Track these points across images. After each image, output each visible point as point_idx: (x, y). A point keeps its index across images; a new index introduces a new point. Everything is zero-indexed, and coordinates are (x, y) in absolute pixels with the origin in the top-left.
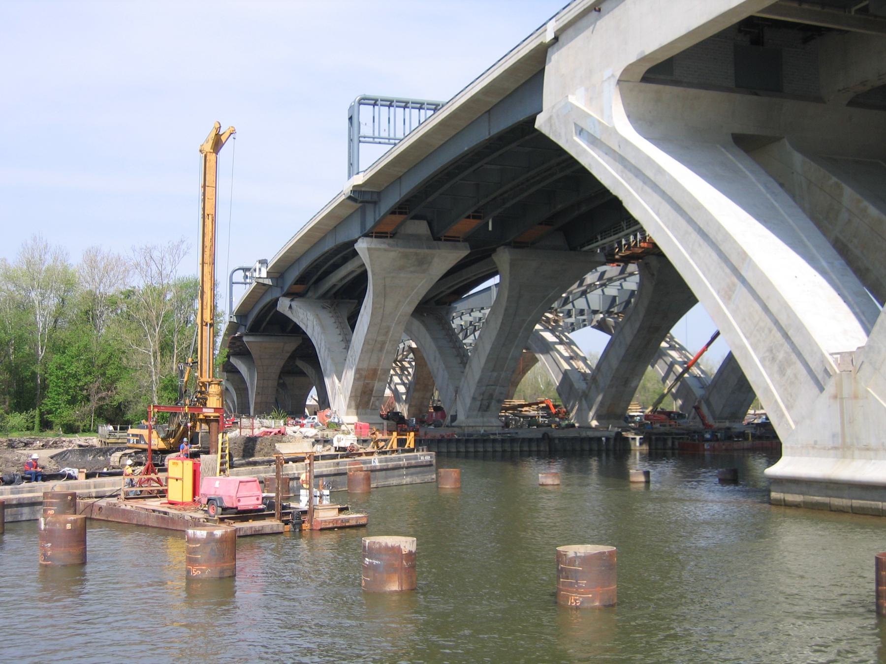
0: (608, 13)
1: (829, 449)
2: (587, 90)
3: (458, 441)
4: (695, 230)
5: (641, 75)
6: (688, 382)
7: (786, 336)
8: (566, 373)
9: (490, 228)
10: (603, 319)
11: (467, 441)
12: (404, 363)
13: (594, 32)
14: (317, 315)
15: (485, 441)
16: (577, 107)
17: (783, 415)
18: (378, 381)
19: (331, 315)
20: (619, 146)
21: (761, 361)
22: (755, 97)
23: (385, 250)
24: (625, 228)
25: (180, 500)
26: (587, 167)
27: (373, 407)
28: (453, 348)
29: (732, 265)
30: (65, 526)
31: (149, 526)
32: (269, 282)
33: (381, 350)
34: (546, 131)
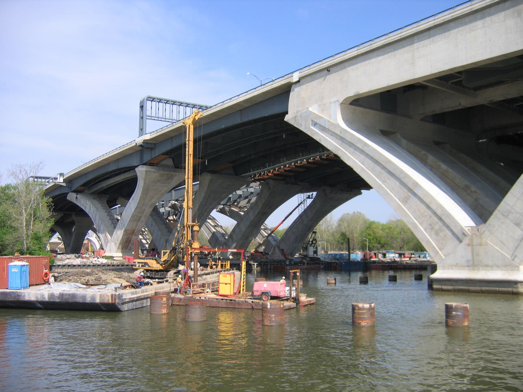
0: (335, 72)
1: (465, 267)
2: (320, 106)
4: (386, 172)
5: (350, 102)
7: (440, 219)
8: (214, 234)
9: (206, 164)
10: (223, 208)
13: (325, 80)
14: (92, 202)
16: (314, 113)
17: (438, 252)
19: (98, 202)
20: (341, 133)
21: (424, 230)
22: (388, 115)
23: (154, 172)
24: (268, 166)
25: (229, 294)
26: (318, 140)
29: (409, 188)
30: (281, 306)
31: (219, 307)
32: (64, 184)
33: (139, 220)
34: (292, 122)
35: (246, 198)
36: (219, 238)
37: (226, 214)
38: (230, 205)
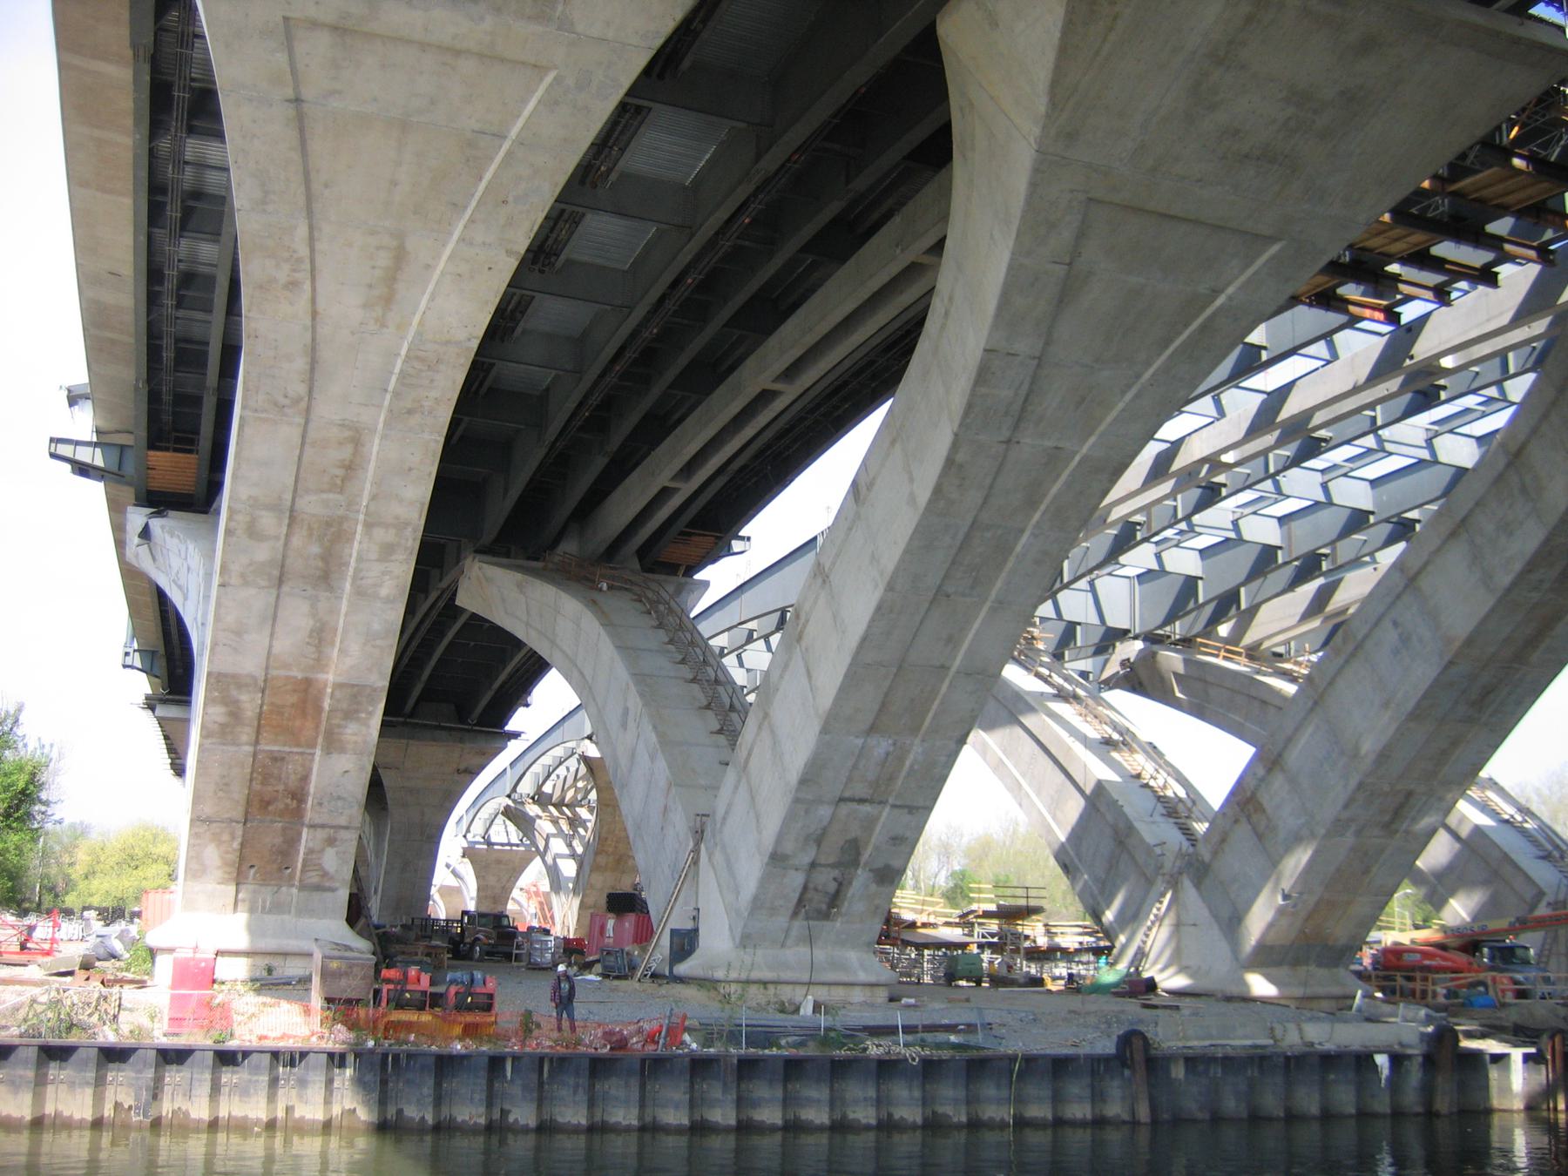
3: (700, 1067)
6: (1494, 837)
10: (1148, 658)
11: (747, 1068)
12: (578, 809)
15: (838, 1070)
18: (328, 750)
27: (313, 878)
28: (694, 680)
33: (326, 575)
35: (1309, 566)
36: (1137, 825)
37: (1165, 697)
38: (1187, 642)
